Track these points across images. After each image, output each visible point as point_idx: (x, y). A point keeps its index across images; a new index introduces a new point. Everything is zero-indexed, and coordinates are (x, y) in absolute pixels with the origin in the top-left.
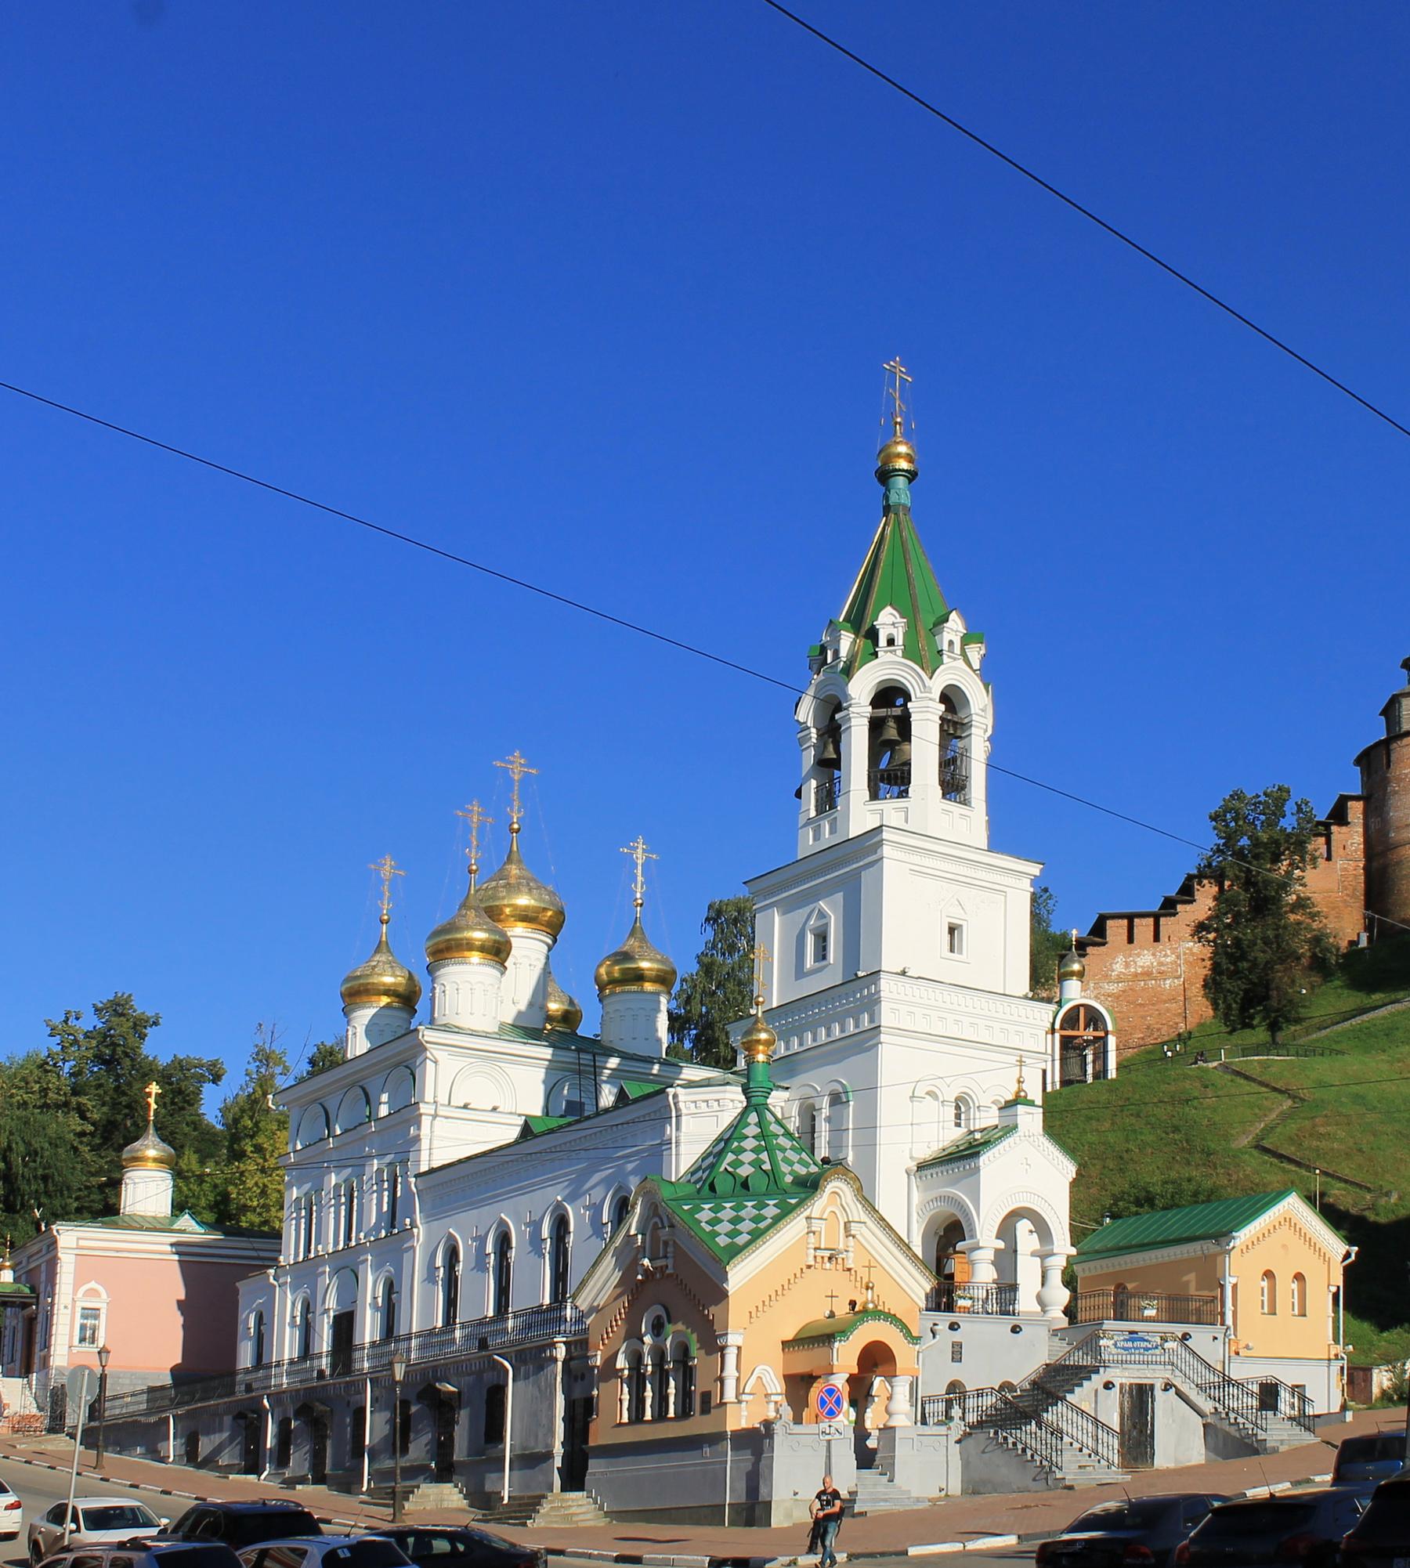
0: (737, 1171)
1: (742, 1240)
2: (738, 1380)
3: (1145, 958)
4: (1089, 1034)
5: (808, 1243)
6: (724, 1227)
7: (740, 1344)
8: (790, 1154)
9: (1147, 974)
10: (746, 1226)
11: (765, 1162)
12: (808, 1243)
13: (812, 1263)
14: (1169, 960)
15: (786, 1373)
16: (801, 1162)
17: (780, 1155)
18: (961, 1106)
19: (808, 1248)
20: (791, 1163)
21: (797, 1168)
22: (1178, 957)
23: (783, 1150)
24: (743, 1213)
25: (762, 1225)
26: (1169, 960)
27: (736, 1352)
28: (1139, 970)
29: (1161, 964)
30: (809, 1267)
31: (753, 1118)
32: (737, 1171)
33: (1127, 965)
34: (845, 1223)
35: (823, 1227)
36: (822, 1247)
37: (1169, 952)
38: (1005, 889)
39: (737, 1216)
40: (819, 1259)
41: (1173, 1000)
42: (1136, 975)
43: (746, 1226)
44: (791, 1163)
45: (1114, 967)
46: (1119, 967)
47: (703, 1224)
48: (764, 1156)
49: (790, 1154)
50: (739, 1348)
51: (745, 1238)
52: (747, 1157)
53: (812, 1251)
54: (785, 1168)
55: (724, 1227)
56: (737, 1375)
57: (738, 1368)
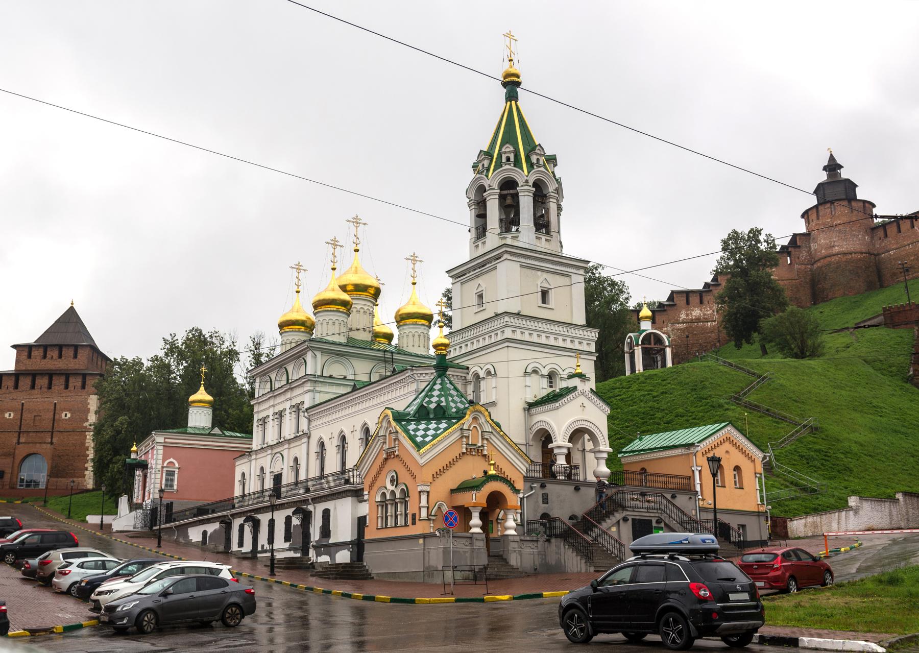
0: (430, 406)
1: (427, 439)
2: (428, 508)
3: (696, 313)
4: (658, 347)
6: (421, 433)
7: (428, 490)
8: (456, 398)
9: (698, 320)
10: (431, 432)
11: (442, 402)
13: (465, 451)
14: (709, 313)
16: (461, 402)
17: (450, 399)
18: (551, 376)
20: (455, 402)
21: (459, 405)
22: (713, 311)
23: (452, 396)
24: (430, 426)
25: (438, 432)
26: (709, 313)
28: (694, 318)
29: (705, 315)
30: (463, 453)
31: (439, 381)
32: (430, 406)
33: (687, 315)
35: (470, 434)
37: (708, 309)
39: (417, 426)
40: (469, 450)
41: (712, 332)
42: (692, 319)
43: (431, 432)
44: (455, 402)
45: (681, 316)
46: (683, 316)
47: (411, 431)
48: (443, 399)
49: (456, 398)
51: (430, 438)
52: (435, 399)
53: (465, 446)
54: (452, 405)
55: (421, 433)
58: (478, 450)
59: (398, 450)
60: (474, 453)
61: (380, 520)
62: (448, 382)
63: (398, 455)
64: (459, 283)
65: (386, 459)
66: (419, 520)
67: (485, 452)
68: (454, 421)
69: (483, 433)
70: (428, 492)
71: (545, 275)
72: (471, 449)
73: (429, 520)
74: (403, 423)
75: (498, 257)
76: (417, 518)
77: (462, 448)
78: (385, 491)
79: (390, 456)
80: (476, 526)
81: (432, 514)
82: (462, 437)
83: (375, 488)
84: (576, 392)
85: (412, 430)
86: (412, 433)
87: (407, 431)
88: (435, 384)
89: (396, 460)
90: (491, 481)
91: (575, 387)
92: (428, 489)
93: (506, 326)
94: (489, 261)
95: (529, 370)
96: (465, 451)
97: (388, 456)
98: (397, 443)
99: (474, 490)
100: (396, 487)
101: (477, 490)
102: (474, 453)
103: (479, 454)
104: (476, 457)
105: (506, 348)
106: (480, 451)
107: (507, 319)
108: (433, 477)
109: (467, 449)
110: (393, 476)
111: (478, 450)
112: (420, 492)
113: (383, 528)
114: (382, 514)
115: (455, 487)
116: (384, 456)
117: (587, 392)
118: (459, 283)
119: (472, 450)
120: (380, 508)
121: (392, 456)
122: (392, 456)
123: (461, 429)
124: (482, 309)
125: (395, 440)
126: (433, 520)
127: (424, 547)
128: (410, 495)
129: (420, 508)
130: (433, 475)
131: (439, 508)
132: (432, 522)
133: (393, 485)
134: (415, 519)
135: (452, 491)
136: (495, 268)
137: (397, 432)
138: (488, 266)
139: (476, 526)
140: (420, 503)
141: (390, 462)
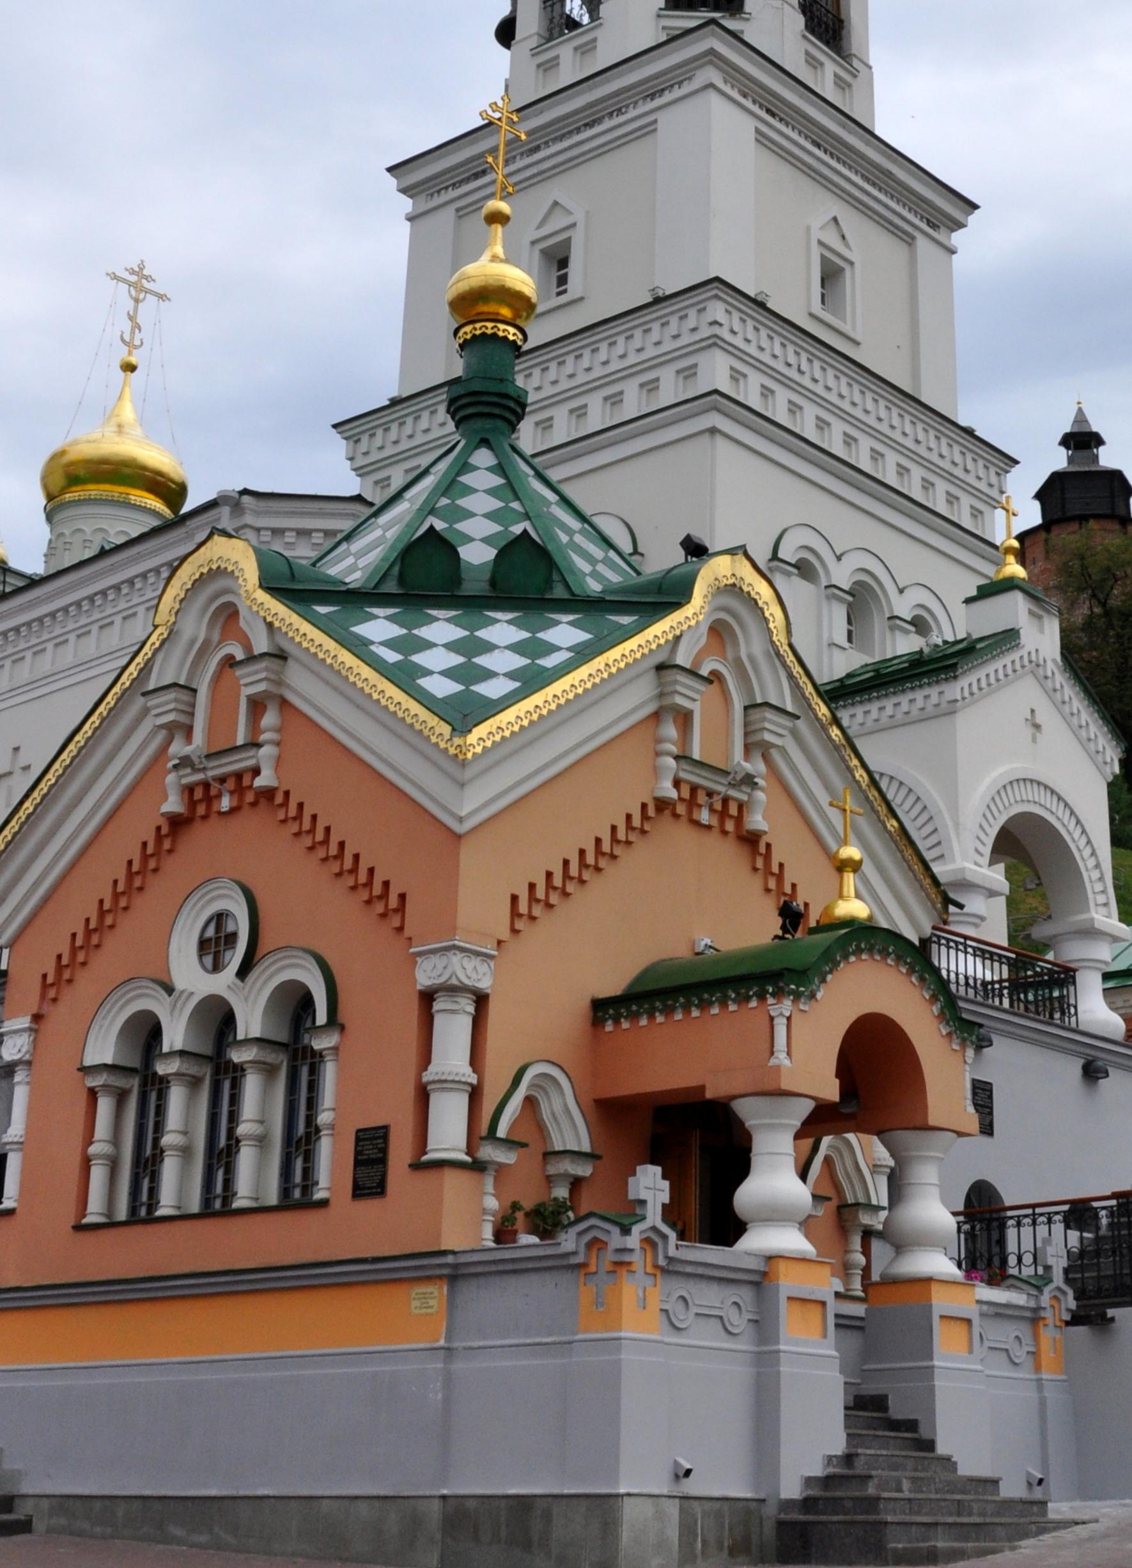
2: (475, 1094)
5: (659, 741)
10: (503, 661)
12: (659, 741)
13: (673, 794)
15: (597, 1097)
19: (658, 754)
25: (549, 662)
27: (471, 1009)
30: (662, 804)
34: (746, 708)
36: (696, 755)
38: (916, 234)
40: (686, 794)
50: (481, 1000)
56: (473, 1079)
57: (476, 1058)
58: (726, 801)
59: (278, 761)
60: (704, 816)
61: (98, 1175)
62: (531, 472)
63: (268, 794)
64: (449, 213)
65: (177, 823)
66: (418, 1166)
67: (757, 821)
68: (625, 620)
69: (755, 715)
70: (481, 1000)
71: (836, 208)
72: (694, 789)
73: (478, 1166)
74: (322, 610)
75: (653, 89)
76: (400, 1153)
77: (656, 772)
78: (158, 1005)
79: (210, 799)
80: (776, 1215)
81: (501, 1132)
82: (656, 716)
83: (86, 985)
84: (1015, 656)
85: (387, 644)
86: (392, 657)
87: (360, 648)
88: (465, 467)
89: (252, 823)
90: (858, 952)
91: (1008, 638)
92: (480, 976)
93: (715, 342)
94: (615, 105)
95: (788, 552)
96: (673, 794)
97: (192, 804)
98: (270, 719)
99: (779, 994)
100: (243, 972)
101: (797, 996)
102: (704, 816)
103: (730, 826)
104: (713, 840)
105: (706, 438)
106: (733, 810)
107: (717, 310)
108: (515, 913)
109: (677, 783)
110: (220, 918)
111: (726, 801)
112: (427, 997)
113: (112, 1225)
114: (116, 1140)
115: (613, 985)
116: (173, 804)
117: (1050, 666)
118: (449, 213)
119: (702, 798)
120: (105, 1106)
121: (225, 803)
122: (225, 803)
123: (661, 668)
124: (563, 299)
125: (257, 706)
126: (500, 1168)
127: (449, 1338)
128: (343, 1015)
129: (423, 1096)
130: (514, 899)
131: (530, 1102)
132: (489, 1183)
133: (217, 967)
134: (382, 1161)
135: (602, 1009)
136: (649, 129)
137: (281, 656)
138: (607, 124)
139: (776, 1215)
140: (426, 1057)
141: (199, 837)
